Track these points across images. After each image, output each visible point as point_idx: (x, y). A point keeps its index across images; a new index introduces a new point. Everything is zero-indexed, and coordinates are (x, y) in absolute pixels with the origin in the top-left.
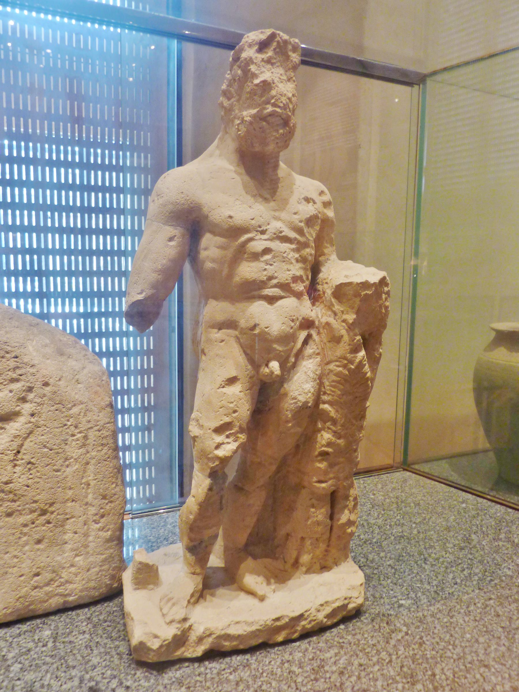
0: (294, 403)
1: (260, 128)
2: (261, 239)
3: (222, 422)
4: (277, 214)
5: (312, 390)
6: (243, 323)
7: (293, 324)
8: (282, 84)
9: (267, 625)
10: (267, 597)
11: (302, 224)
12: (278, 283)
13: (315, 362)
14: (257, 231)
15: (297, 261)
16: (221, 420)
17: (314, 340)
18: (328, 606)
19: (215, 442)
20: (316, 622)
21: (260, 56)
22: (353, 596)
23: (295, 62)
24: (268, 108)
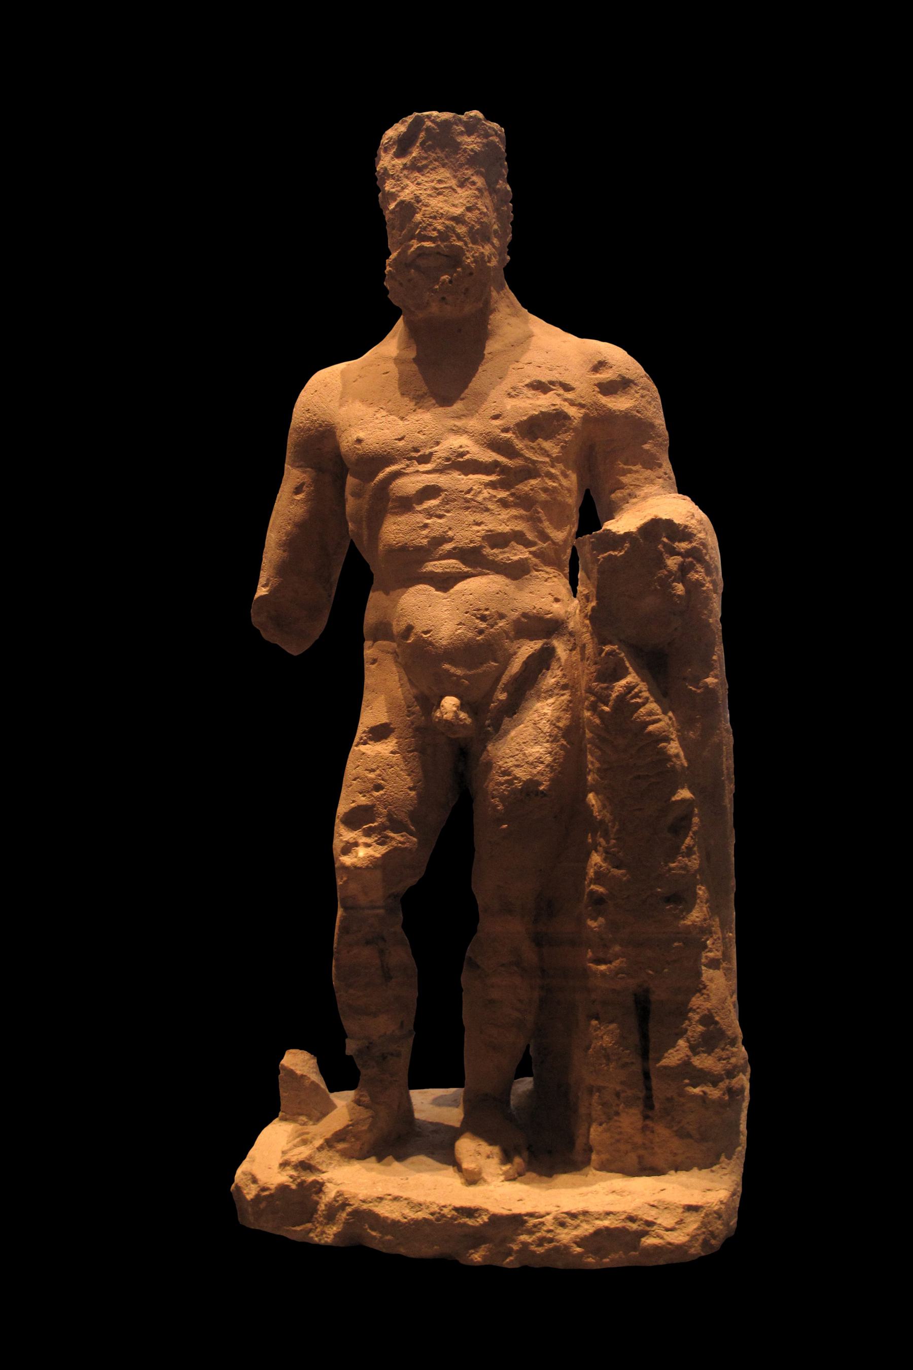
0: (507, 782)
1: (409, 281)
2: (418, 471)
3: (353, 805)
4: (459, 423)
5: (548, 759)
6: (398, 627)
7: (483, 625)
8: (441, 197)
9: (444, 1216)
10: (485, 1181)
11: (508, 435)
12: (454, 548)
13: (558, 703)
14: (410, 459)
15: (504, 503)
16: (354, 801)
17: (559, 659)
18: (587, 1222)
19: (341, 841)
20: (552, 1245)
21: (399, 162)
22: (658, 1221)
23: (472, 150)
24: (412, 245)
